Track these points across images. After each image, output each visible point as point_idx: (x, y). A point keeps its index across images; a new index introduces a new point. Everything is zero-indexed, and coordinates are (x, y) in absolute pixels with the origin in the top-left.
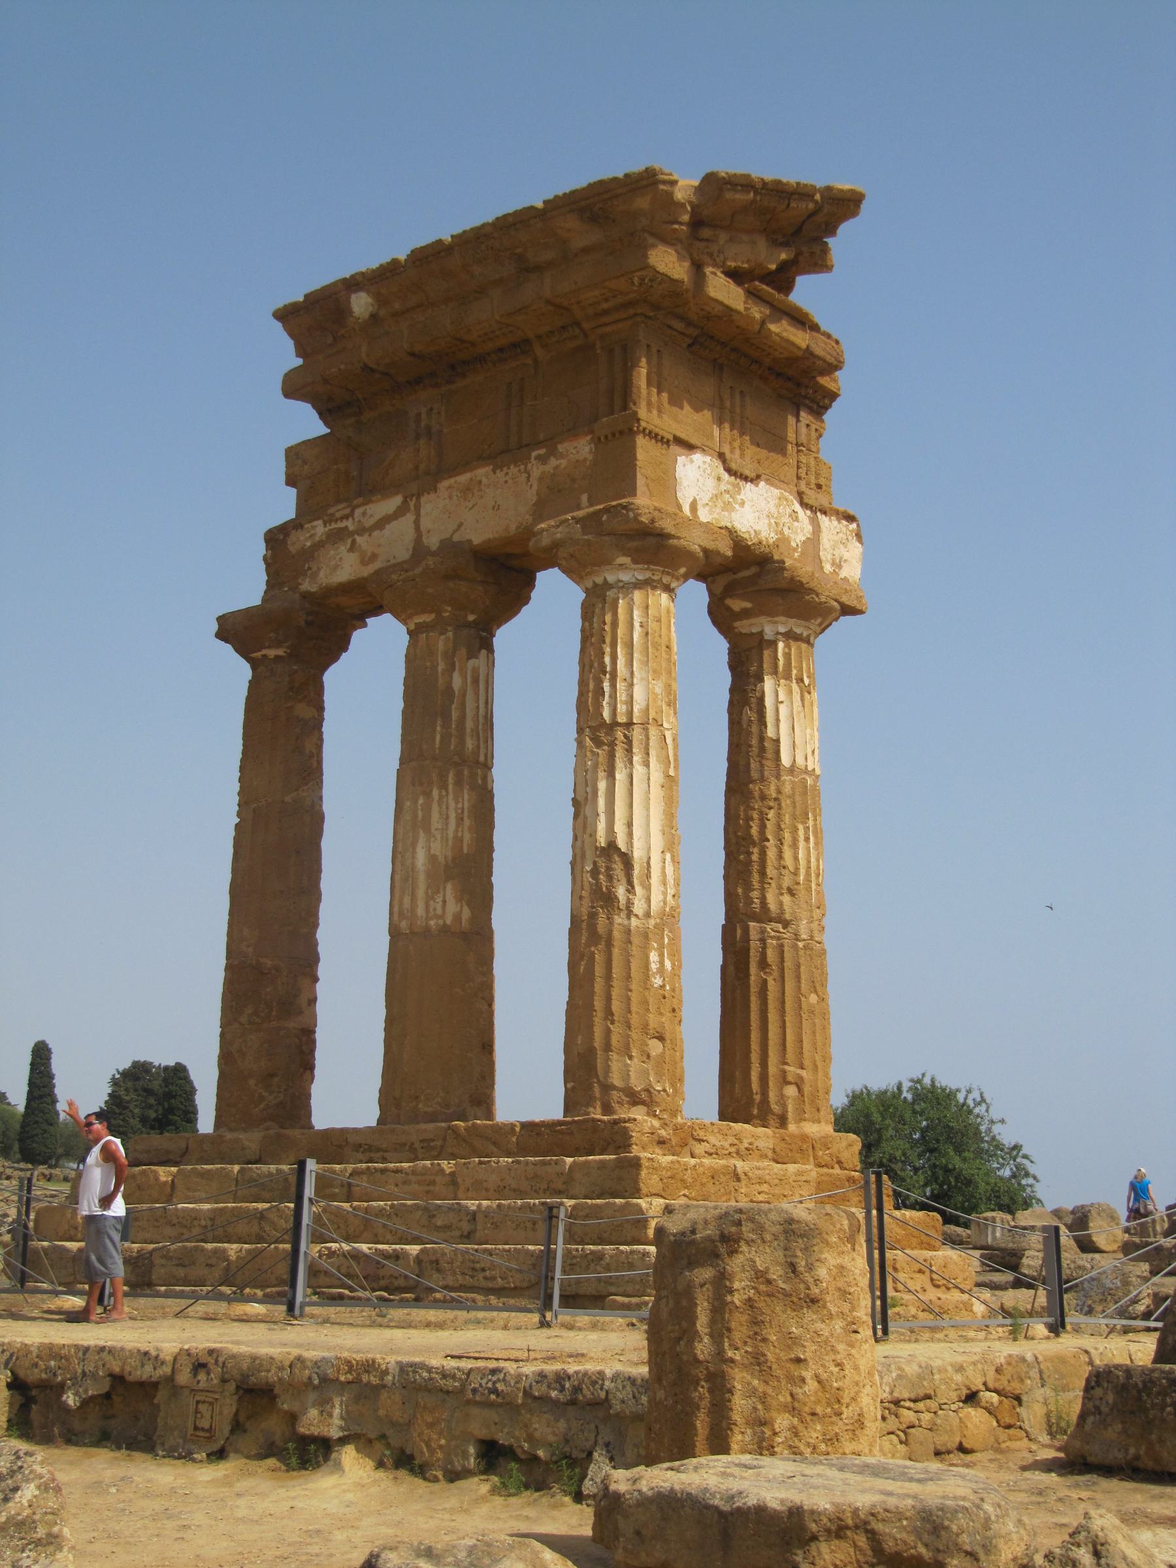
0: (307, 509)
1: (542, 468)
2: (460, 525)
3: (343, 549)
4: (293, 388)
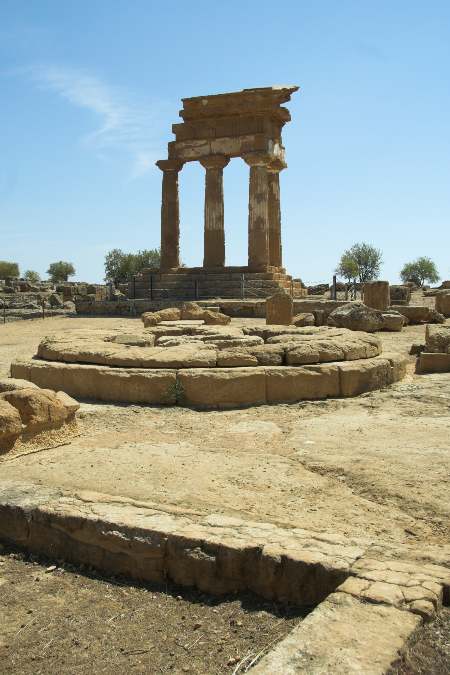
0: (178, 140)
1: (242, 141)
2: (222, 149)
3: (190, 150)
4: (181, 114)
